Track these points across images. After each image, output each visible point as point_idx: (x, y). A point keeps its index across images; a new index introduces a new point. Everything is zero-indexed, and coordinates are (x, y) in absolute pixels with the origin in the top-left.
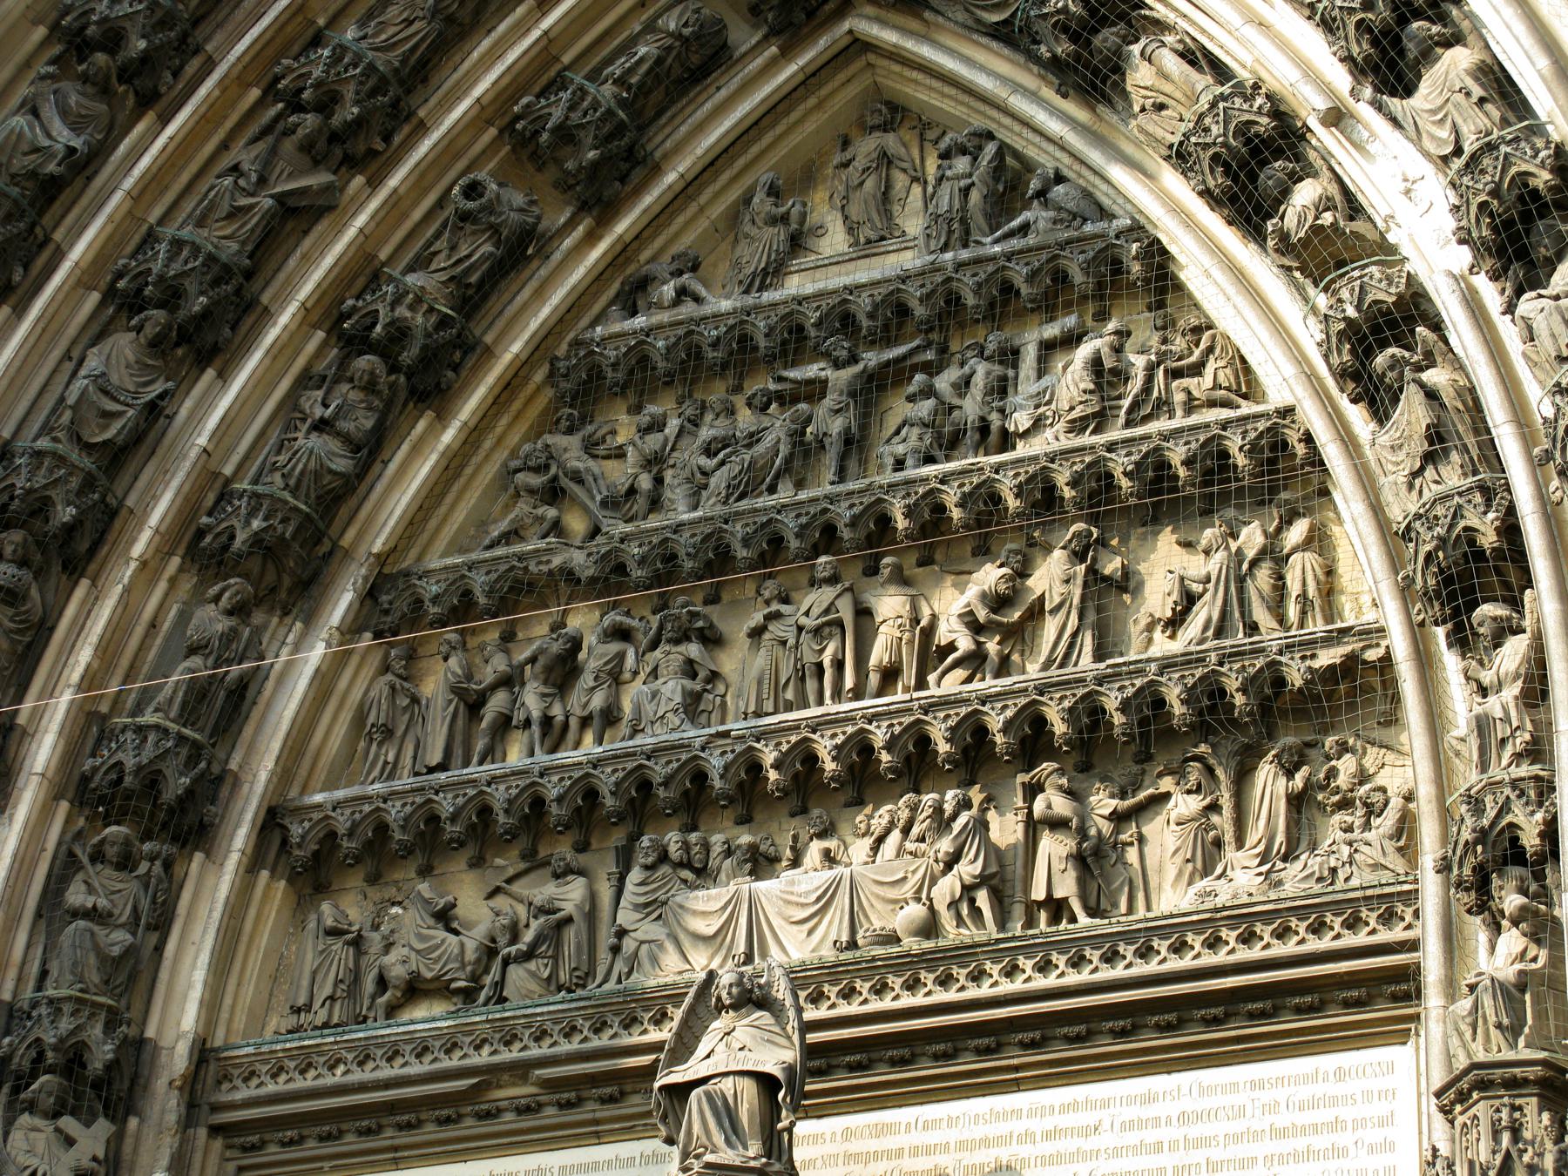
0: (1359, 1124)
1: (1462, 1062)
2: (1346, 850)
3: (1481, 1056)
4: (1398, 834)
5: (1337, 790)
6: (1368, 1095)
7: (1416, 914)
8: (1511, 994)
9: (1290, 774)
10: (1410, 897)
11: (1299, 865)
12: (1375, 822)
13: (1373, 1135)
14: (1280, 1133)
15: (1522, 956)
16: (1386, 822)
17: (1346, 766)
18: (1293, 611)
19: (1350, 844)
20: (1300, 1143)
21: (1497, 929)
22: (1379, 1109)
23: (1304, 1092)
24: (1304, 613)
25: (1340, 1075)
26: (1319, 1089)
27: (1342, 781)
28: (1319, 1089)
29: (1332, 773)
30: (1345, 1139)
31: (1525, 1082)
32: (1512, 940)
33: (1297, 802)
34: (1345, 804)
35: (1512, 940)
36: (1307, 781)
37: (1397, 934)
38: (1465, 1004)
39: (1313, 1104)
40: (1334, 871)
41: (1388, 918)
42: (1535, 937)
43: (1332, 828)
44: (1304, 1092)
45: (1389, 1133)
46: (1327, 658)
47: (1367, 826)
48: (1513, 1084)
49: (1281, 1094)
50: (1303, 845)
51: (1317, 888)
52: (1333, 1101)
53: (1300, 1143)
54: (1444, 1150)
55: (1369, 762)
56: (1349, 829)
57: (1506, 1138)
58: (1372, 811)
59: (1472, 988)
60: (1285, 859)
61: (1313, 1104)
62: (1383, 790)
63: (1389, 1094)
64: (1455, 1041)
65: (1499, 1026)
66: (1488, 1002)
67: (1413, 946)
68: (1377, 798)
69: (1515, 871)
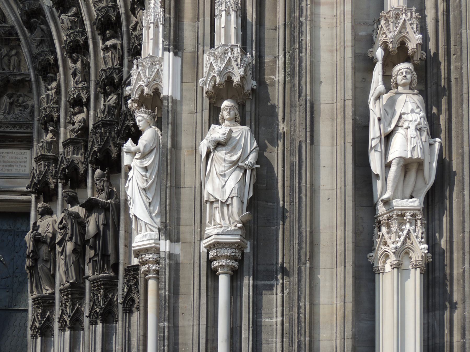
0: (20, 162)
1: (40, 154)
2: (20, 114)
3: (43, 153)
4: (30, 113)
5: (19, 103)
6: (22, 158)
7: (33, 128)
8: (50, 144)
9: (10, 98)
10: (32, 125)
11: (11, 116)
12: (26, 110)
13: (23, 164)
14: (6, 162)
15: (52, 138)
16: (28, 110)
17: (21, 99)
18: (11, 68)
19: (21, 113)
20: (9, 164)
21: (47, 133)
22: (25, 160)
23: (10, 155)
24: (14, 69)
25: (17, 153)
26: (13, 155)
27: (20, 101)
28: (13, 155)
29: (18, 100)
30: (18, 164)
31: (51, 159)
32: (50, 135)
33: (11, 104)
34: (20, 106)
35: (50, 135)
36: (13, 101)
37: (29, 130)
38: (41, 144)
39: (12, 157)
40: (18, 118)
41: (27, 128)
42: (54, 135)
43: (17, 110)
44: (10, 155)
45: (26, 164)
46: (18, 78)
47: (24, 111)
48: (48, 159)
49: (6, 155)
50: (12, 112)
51: (14, 120)
52: (15, 158)
53: (9, 164)
54: (35, 168)
55: (26, 99)
56: (21, 111)
57: (46, 167)
58: (26, 108)
59: (42, 142)
60: (8, 114)
61: (12, 157)
62: (28, 105)
63: (26, 158)
64: (38, 150)
65: (47, 149)
66: (45, 145)
67: (32, 133)
68: (26, 106)
69: (52, 123)
